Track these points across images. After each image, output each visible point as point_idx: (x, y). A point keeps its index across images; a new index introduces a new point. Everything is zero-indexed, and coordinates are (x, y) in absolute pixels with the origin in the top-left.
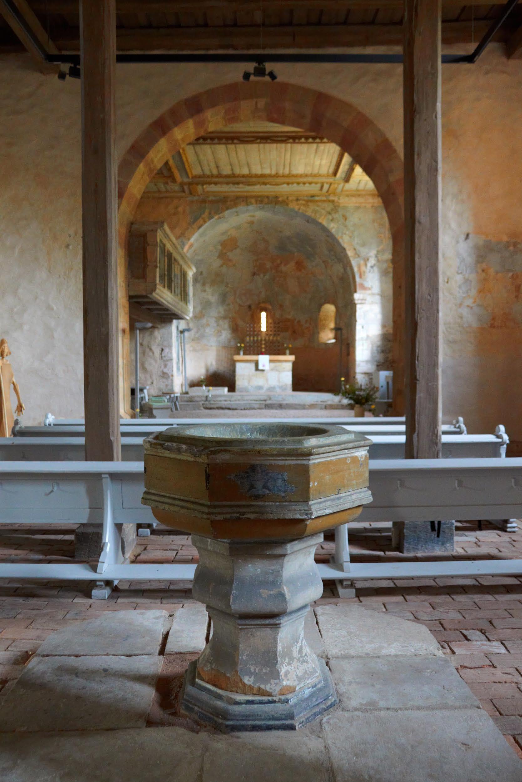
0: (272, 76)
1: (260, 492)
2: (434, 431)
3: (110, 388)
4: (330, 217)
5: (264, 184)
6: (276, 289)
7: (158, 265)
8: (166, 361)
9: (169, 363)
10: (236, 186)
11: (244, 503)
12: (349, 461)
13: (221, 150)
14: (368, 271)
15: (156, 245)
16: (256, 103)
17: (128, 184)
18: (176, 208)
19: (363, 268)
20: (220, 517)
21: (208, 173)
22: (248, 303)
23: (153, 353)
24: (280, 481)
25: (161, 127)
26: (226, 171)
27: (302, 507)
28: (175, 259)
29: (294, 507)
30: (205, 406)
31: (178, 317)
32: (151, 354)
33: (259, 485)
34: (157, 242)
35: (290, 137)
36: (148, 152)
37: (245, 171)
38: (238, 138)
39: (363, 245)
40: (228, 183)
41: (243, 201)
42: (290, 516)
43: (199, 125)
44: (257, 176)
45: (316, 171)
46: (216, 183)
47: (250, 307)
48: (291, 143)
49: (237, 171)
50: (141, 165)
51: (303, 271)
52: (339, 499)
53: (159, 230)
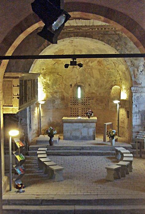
4: (117, 43)
6: (86, 75)
19: (136, 72)
22: (70, 83)
41: (67, 35)
47: (71, 85)
51: (102, 66)
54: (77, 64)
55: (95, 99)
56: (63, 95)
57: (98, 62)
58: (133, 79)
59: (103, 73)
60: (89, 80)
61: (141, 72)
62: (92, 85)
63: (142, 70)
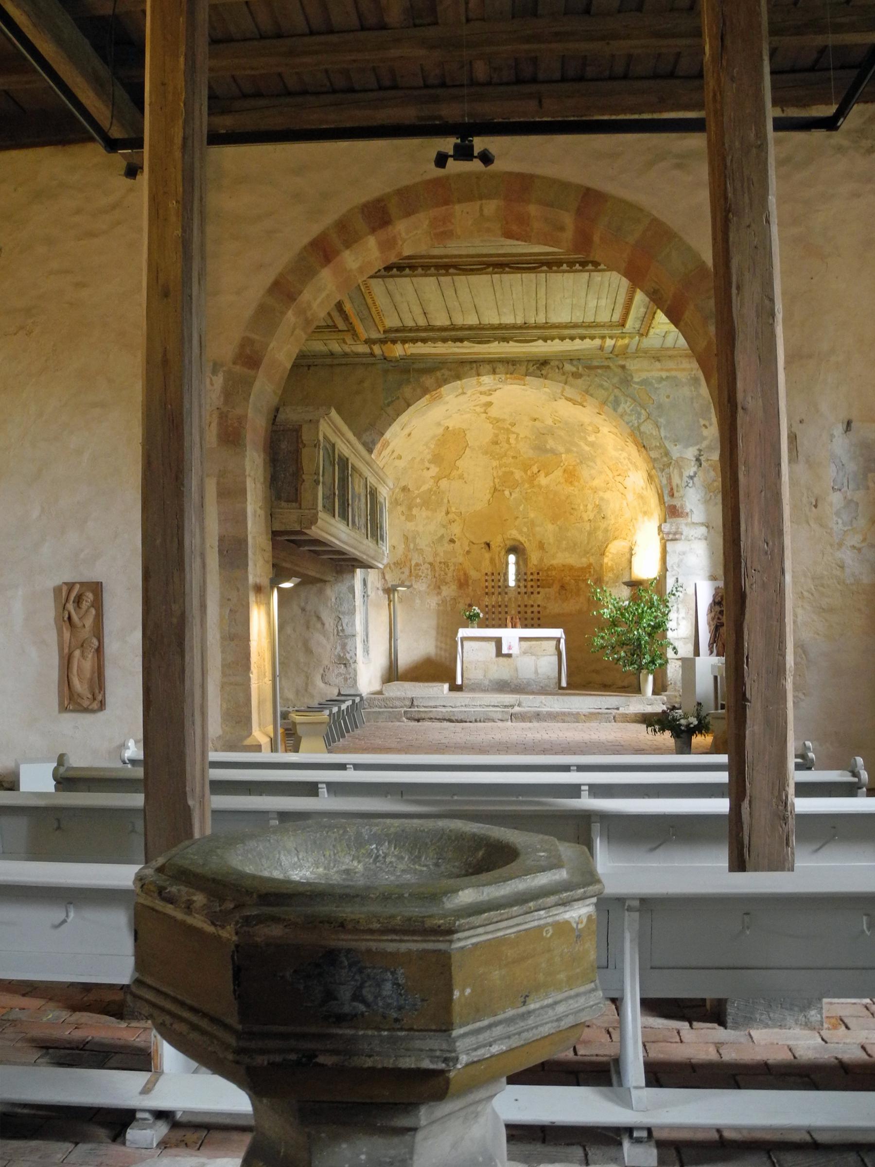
0: (486, 158)
1: (347, 1009)
2: (780, 795)
3: (187, 712)
5: (506, 340)
7: (321, 479)
8: (344, 637)
9: (349, 642)
10: (458, 344)
11: (313, 1029)
12: (548, 933)
13: (428, 284)
14: (684, 484)
15: (316, 445)
16: (481, 209)
17: (268, 345)
18: (361, 382)
19: (676, 480)
20: (261, 1060)
21: (410, 323)
23: (323, 624)
24: (388, 986)
25: (323, 251)
26: (441, 320)
27: (435, 1043)
28: (353, 467)
29: (418, 1044)
30: (409, 715)
31: (366, 566)
32: (319, 626)
33: (345, 993)
34: (319, 441)
35: (543, 264)
36: (301, 292)
37: (472, 320)
38: (455, 266)
39: (676, 441)
40: (445, 340)
42: (407, 1063)
43: (387, 245)
44: (493, 327)
45: (590, 319)
46: (424, 341)
48: (546, 272)
49: (459, 320)
50: (290, 313)
51: (576, 484)
52: (524, 1016)
53: (322, 421)
54: (476, 154)
55: (556, 587)
56: (465, 574)
57: (565, 471)
58: (666, 498)
59: (581, 507)
60: (538, 529)
61: (691, 478)
62: (549, 544)
63: (692, 474)
